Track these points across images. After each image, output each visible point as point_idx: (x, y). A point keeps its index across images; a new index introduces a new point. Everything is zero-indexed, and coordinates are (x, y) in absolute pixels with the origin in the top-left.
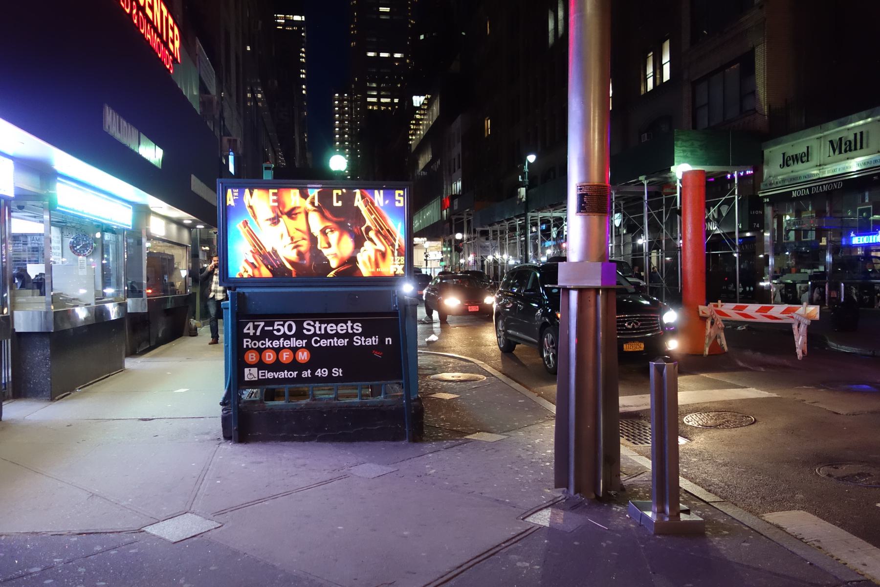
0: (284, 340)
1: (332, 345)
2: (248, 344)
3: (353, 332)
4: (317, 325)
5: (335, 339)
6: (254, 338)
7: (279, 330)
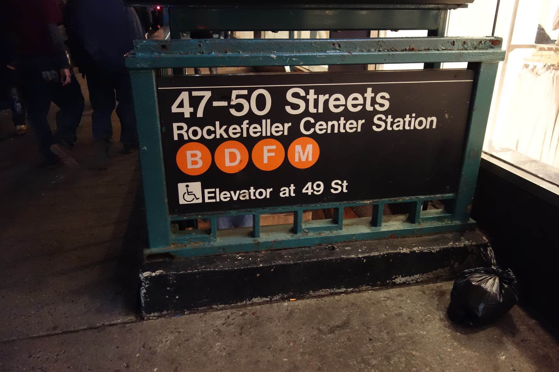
0: (250, 124)
1: (336, 131)
3: (374, 108)
4: (312, 96)
5: (342, 121)
6: (193, 121)
7: (239, 107)
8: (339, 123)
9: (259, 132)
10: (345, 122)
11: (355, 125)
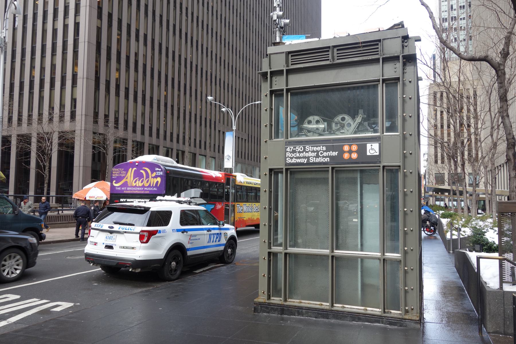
0: (305, 153)
2: (289, 155)
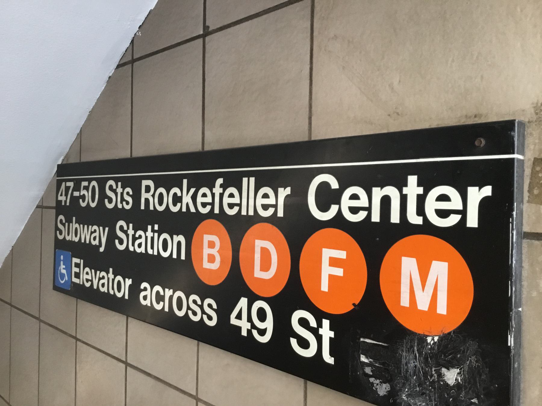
0: (224, 187)
1: (395, 218)
8: (404, 193)
9: (272, 206)
10: (420, 191)
11: (456, 203)
